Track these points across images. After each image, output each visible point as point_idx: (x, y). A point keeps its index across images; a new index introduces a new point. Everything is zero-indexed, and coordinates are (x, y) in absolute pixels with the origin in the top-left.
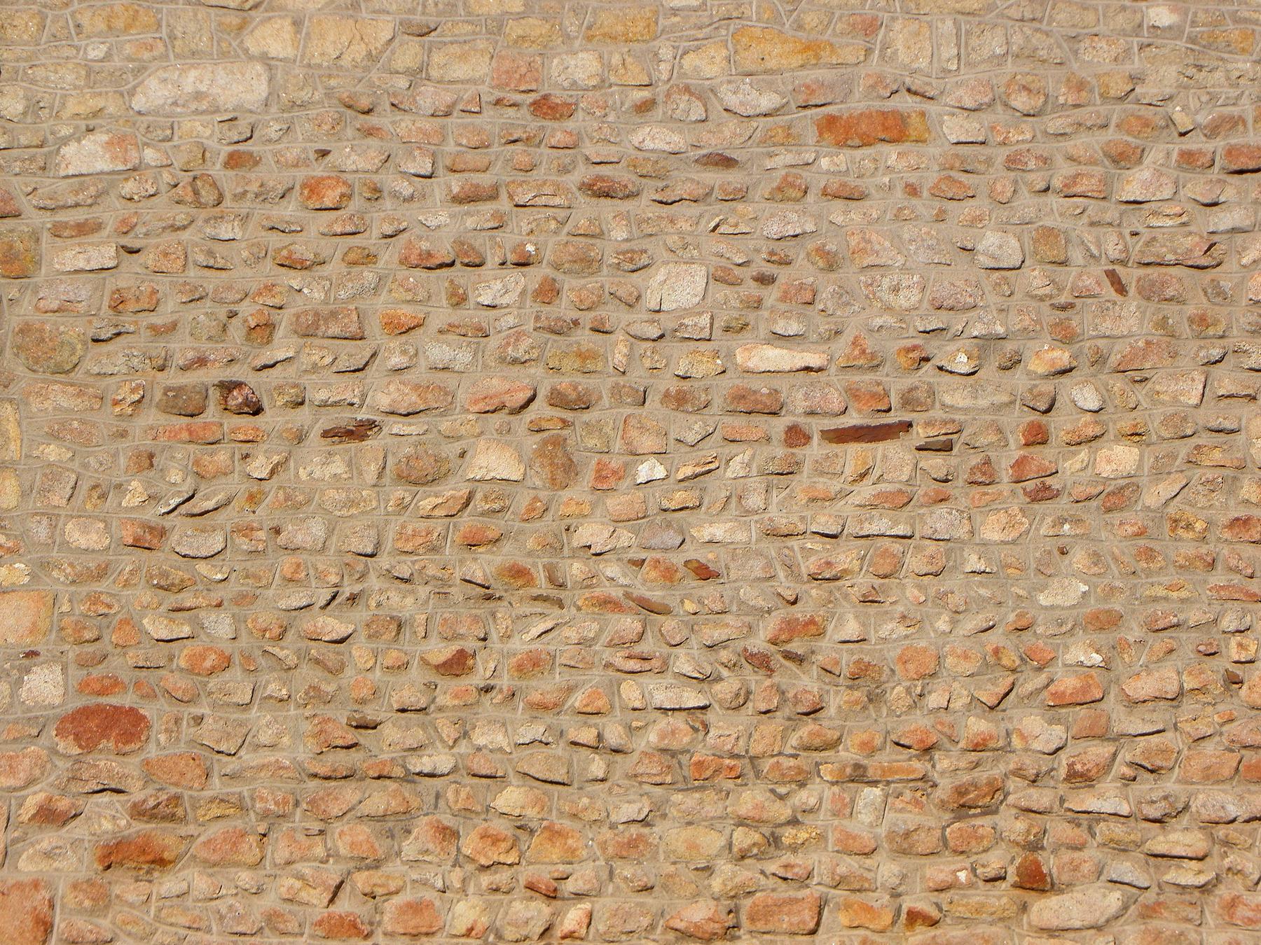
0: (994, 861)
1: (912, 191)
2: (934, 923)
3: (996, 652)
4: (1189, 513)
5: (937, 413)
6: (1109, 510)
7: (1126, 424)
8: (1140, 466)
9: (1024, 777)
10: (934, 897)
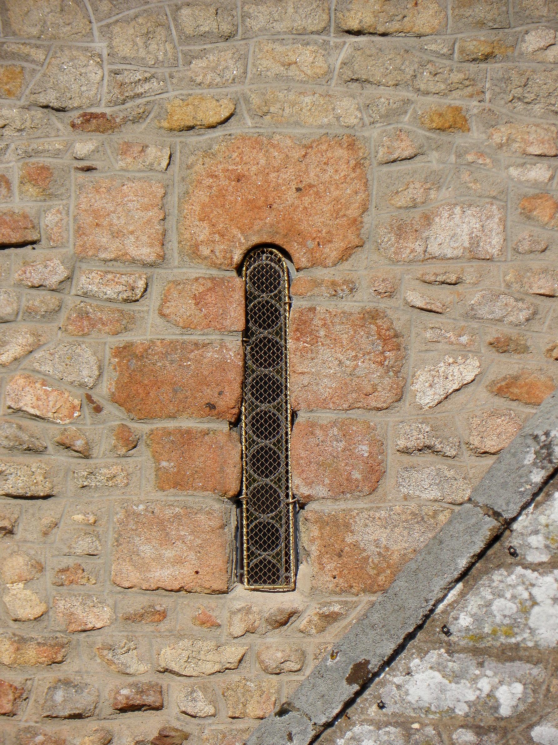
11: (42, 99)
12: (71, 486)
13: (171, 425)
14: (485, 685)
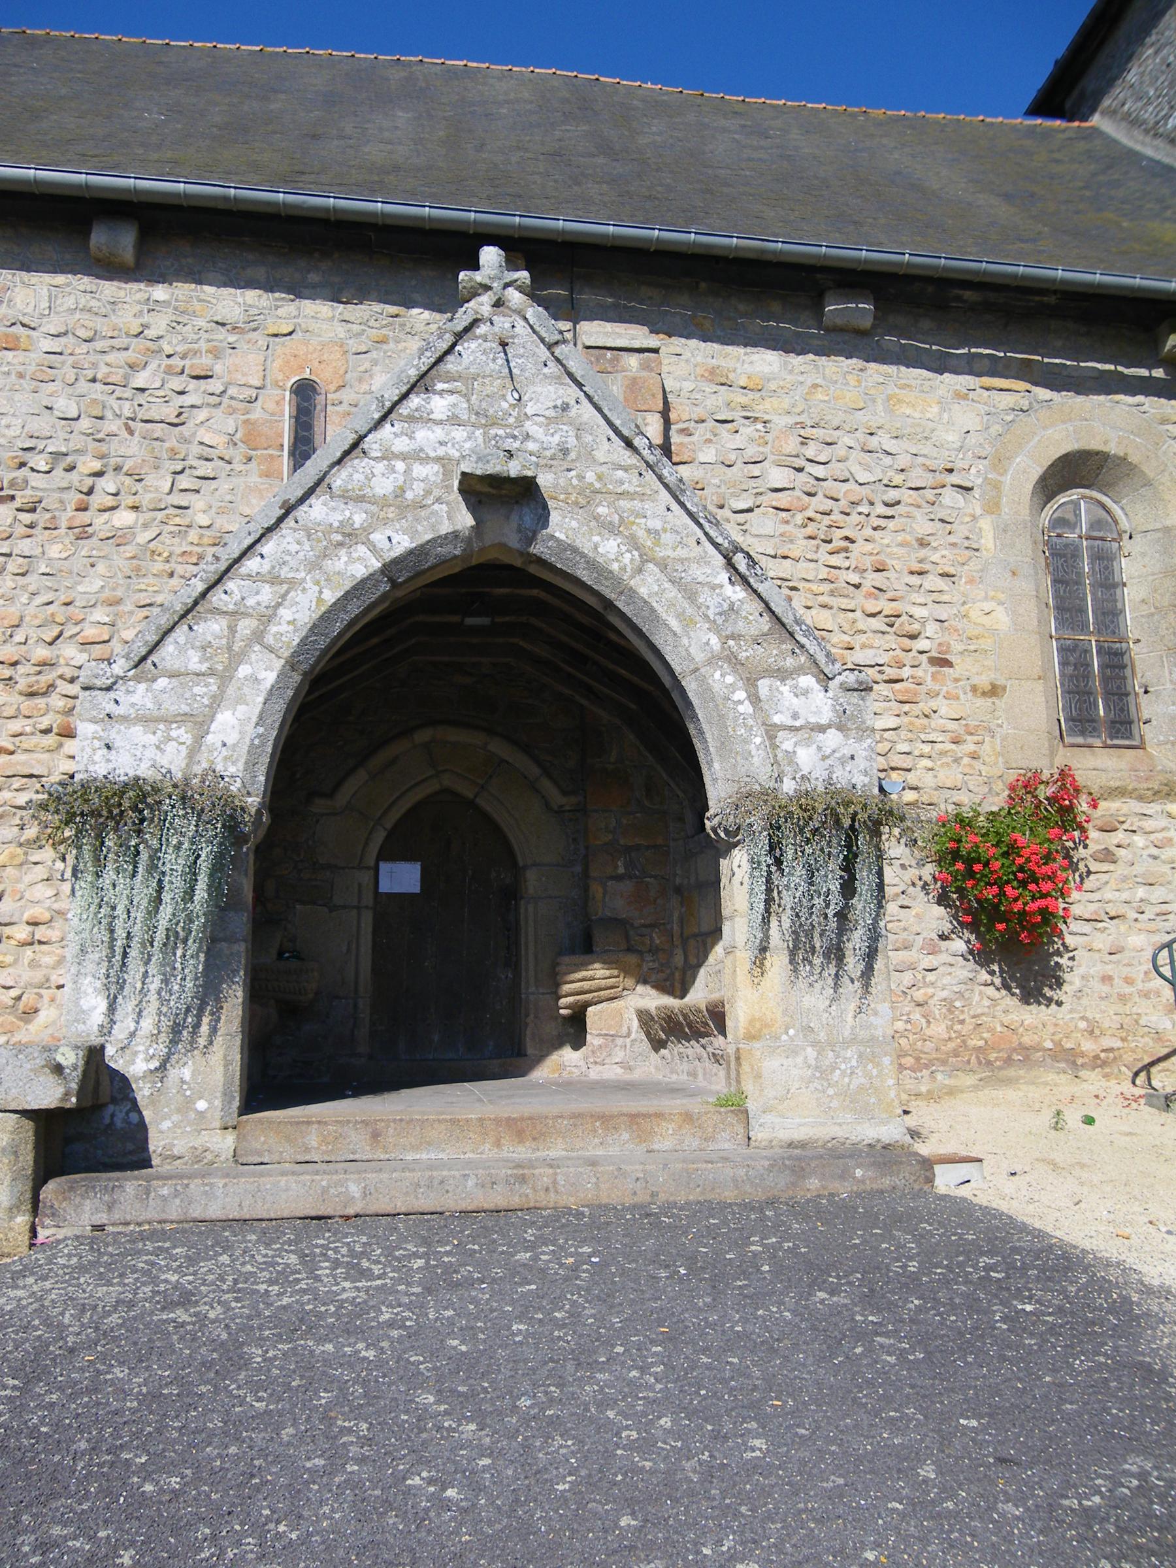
0: (45, 723)
1: (21, 376)
2: (12, 753)
3: (52, 615)
4: (160, 549)
5: (29, 492)
6: (118, 545)
7: (130, 500)
8: (136, 523)
9: (65, 680)
10: (12, 739)
11: (215, 319)
12: (223, 475)
13: (265, 452)
14: (347, 513)
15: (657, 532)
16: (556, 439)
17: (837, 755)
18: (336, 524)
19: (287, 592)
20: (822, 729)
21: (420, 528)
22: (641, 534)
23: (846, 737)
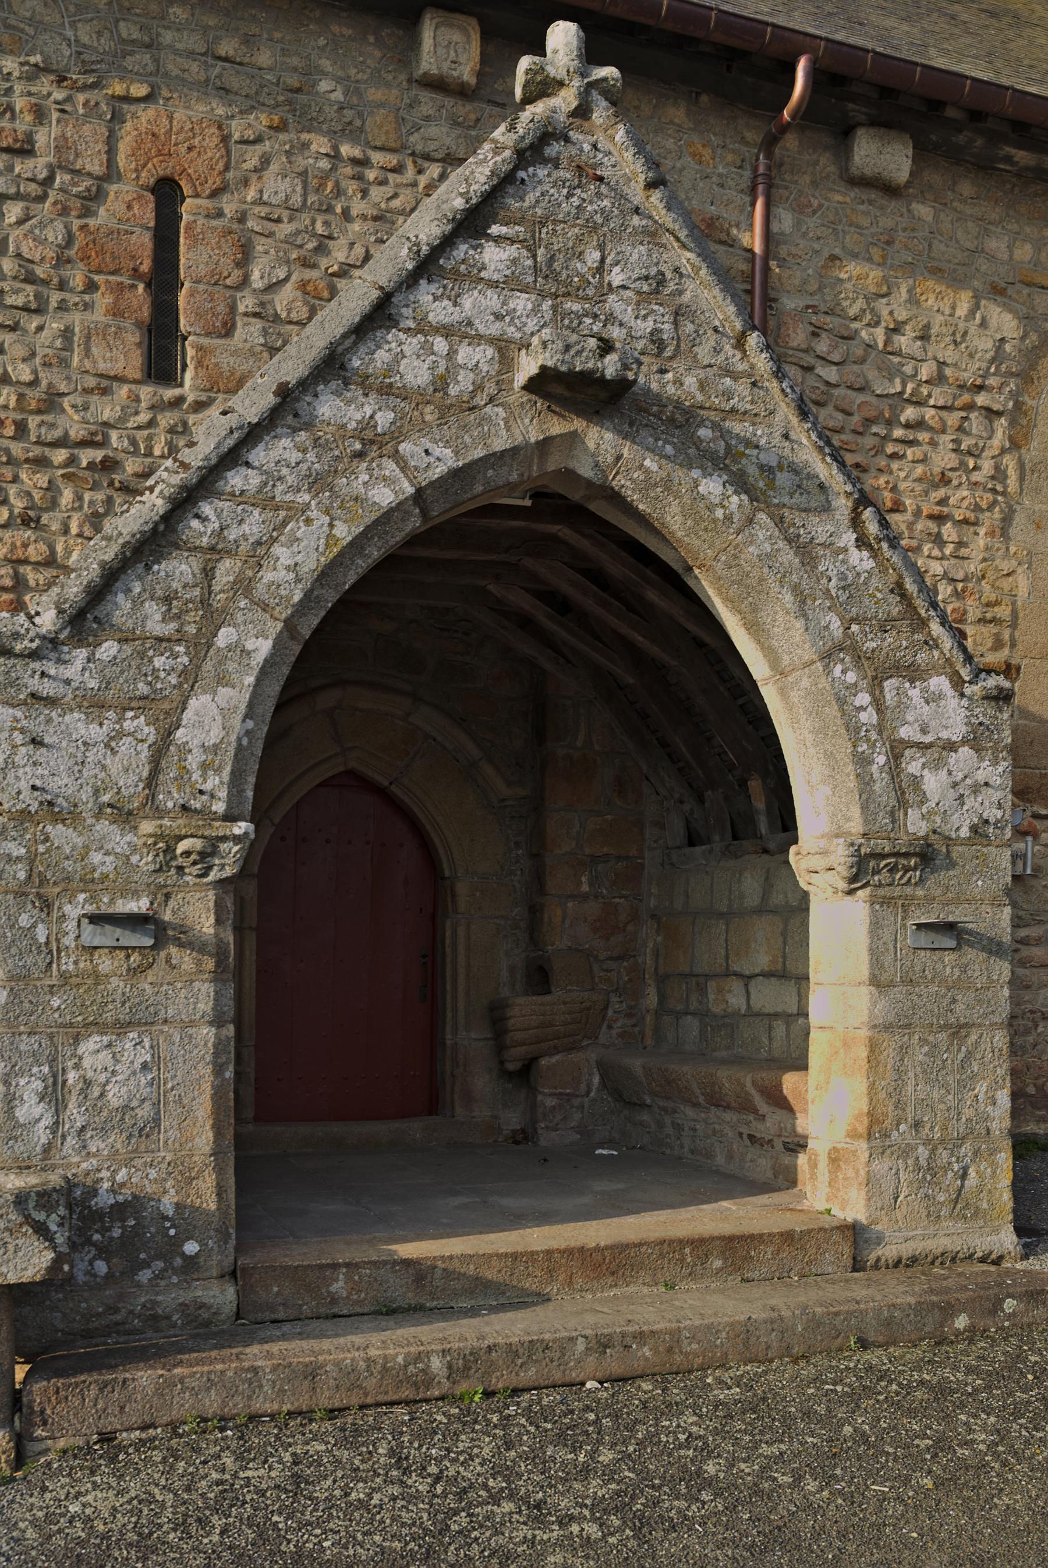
14: (368, 410)
15: (770, 469)
16: (649, 325)
17: (968, 781)
18: (353, 425)
19: (284, 523)
20: (951, 747)
21: (467, 439)
22: (752, 470)
23: (981, 759)
